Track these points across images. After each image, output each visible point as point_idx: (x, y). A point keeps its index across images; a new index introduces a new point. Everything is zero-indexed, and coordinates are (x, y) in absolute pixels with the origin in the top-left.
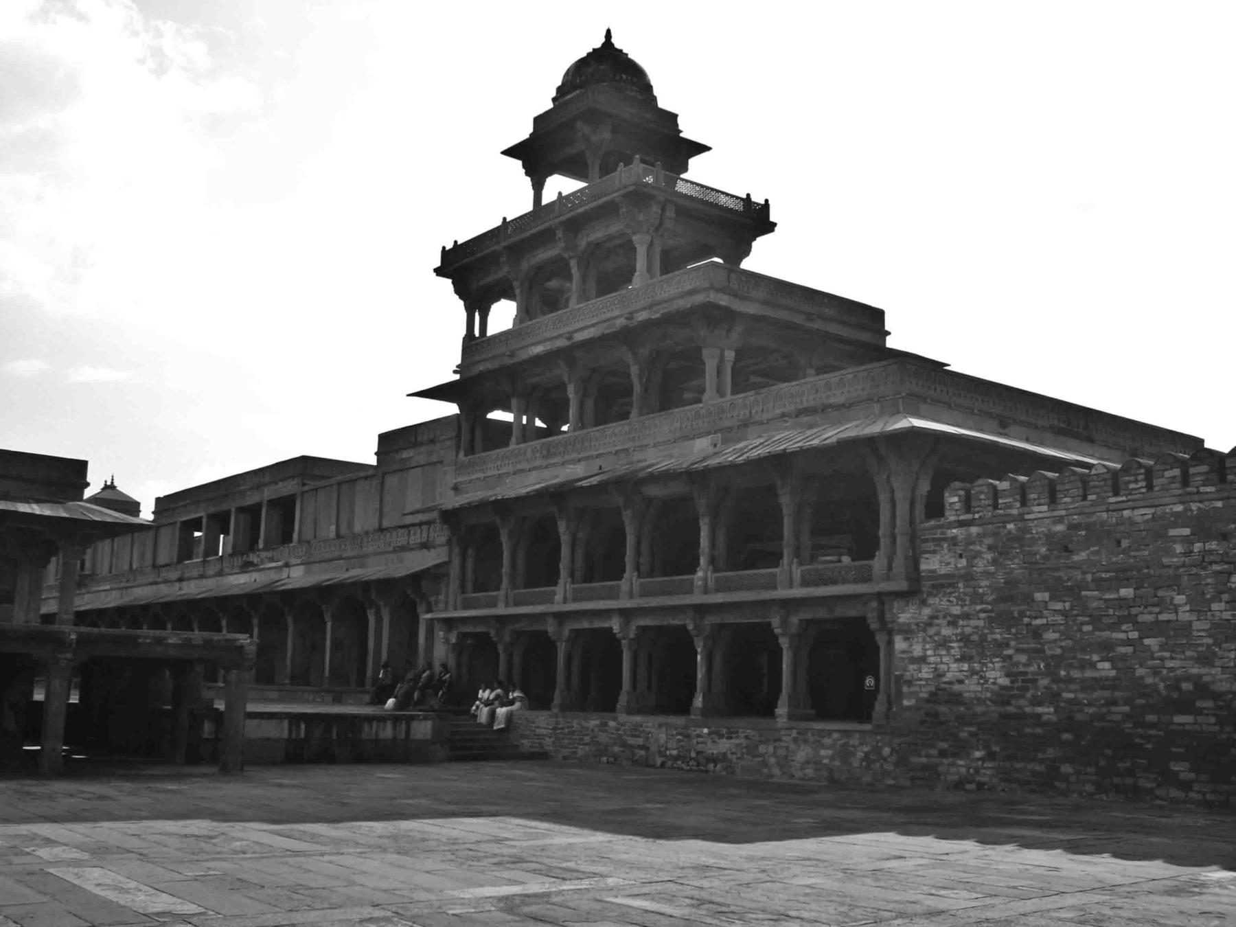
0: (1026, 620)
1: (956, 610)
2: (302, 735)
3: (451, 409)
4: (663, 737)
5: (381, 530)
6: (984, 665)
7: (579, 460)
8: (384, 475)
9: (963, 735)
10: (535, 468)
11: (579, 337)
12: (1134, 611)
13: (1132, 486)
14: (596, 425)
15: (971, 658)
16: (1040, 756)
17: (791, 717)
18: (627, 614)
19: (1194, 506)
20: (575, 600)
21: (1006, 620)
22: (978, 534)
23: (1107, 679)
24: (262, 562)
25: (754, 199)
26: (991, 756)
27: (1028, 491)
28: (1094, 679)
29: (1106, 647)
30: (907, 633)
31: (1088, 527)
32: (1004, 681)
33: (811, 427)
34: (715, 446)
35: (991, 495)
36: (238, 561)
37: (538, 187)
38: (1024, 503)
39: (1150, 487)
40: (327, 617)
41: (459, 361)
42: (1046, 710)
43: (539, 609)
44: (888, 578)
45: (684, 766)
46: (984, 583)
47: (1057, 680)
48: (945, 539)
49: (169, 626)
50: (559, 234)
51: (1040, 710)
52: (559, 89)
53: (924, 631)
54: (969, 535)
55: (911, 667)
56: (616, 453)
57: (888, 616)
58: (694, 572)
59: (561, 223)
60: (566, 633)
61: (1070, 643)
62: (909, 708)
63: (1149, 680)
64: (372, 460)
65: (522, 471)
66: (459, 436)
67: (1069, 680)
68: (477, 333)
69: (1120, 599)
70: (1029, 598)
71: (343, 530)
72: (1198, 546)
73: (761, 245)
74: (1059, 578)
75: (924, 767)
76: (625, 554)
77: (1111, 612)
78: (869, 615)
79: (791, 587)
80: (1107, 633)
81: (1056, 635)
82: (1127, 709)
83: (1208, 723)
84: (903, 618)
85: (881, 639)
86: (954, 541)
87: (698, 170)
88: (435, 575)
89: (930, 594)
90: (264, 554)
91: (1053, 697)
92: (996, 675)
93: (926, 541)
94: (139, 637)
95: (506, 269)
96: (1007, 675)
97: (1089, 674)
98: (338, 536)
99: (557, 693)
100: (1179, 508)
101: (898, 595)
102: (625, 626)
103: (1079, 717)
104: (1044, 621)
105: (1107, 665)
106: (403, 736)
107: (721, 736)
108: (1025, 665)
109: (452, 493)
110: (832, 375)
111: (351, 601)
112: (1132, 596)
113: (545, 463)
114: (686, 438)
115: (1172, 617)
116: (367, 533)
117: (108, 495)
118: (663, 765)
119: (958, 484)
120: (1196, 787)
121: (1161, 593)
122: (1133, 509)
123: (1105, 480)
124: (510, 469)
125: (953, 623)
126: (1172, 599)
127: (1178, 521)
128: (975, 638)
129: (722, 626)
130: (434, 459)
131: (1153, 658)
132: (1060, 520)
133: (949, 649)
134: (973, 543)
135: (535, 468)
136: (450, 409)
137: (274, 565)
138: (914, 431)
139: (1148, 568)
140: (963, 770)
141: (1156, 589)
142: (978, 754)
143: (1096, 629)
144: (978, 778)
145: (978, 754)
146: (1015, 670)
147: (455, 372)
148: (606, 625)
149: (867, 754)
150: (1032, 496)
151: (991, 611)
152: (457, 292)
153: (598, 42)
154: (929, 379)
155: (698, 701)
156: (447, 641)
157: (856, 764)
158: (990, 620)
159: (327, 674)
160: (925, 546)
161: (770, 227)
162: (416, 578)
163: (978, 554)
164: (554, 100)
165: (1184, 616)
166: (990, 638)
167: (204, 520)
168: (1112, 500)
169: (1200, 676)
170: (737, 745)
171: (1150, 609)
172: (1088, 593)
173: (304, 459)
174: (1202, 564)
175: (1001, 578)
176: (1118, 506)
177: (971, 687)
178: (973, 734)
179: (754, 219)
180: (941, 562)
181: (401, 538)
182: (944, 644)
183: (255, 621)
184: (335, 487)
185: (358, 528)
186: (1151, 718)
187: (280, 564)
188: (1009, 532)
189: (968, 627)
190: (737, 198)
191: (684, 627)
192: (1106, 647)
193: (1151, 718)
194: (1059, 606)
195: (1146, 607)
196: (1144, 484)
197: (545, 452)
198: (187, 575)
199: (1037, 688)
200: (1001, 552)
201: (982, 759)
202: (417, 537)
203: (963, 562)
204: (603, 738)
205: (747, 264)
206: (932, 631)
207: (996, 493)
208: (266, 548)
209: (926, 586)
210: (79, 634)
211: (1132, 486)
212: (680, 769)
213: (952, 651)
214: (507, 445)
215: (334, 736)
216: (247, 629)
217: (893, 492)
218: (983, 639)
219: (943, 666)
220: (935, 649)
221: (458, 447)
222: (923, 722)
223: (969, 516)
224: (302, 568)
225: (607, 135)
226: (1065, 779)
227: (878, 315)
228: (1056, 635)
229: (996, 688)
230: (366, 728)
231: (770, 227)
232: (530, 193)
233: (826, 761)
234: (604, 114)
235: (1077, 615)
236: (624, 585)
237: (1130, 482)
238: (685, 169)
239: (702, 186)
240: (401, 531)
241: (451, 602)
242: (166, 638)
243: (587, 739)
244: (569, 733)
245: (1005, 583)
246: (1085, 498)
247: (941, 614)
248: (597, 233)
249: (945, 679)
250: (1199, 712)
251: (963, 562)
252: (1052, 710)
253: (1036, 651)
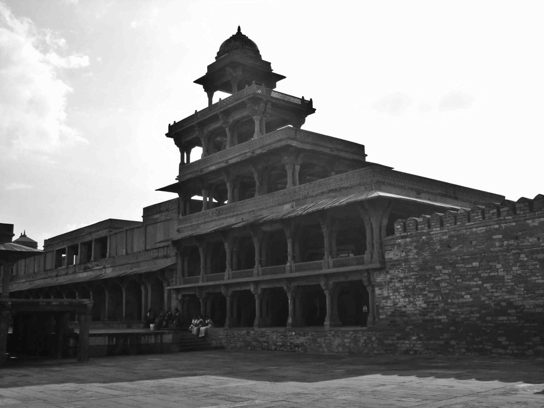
0: (432, 278)
1: (402, 275)
2: (114, 343)
3: (175, 196)
4: (274, 337)
5: (146, 250)
6: (415, 299)
7: (233, 216)
8: (146, 226)
9: (407, 330)
10: (215, 220)
11: (231, 162)
12: (479, 272)
13: (476, 217)
14: (240, 200)
15: (409, 296)
16: (441, 337)
17: (331, 325)
18: (257, 283)
19: (503, 225)
20: (233, 278)
22: (410, 242)
23: (469, 302)
24: (93, 267)
25: (305, 99)
26: (419, 339)
27: (431, 222)
28: (463, 303)
30: (381, 286)
31: (458, 236)
32: (424, 305)
33: (334, 197)
34: (293, 207)
35: (415, 225)
36: (82, 267)
37: (210, 97)
38: (429, 227)
39: (484, 218)
40: (123, 290)
41: (178, 174)
42: (443, 317)
43: (218, 283)
44: (371, 262)
45: (285, 350)
46: (413, 263)
48: (395, 244)
49: (52, 297)
50: (220, 117)
51: (440, 317)
52: (218, 53)
53: (388, 285)
54: (406, 243)
55: (383, 301)
56: (249, 212)
57: (372, 279)
58: (286, 263)
59: (221, 112)
60: (230, 292)
61: (452, 287)
62: (382, 319)
63: (487, 302)
64: (141, 220)
65: (207, 222)
66: (179, 207)
67: (452, 304)
68: (185, 162)
69: (473, 267)
70: (433, 268)
71: (129, 252)
72: (506, 243)
73: (309, 119)
74: (446, 260)
75: (390, 345)
76: (255, 257)
77: (469, 273)
78: (363, 279)
79: (329, 268)
80: (468, 283)
81: (446, 284)
82: (478, 315)
84: (379, 280)
85: (369, 289)
86: (399, 245)
87: (281, 87)
88: (171, 269)
89: (390, 269)
90: (93, 263)
91: (445, 311)
92: (420, 303)
93: (388, 245)
94: (40, 302)
95: (197, 133)
96: (425, 303)
97: (461, 300)
98: (127, 254)
99: (227, 319)
100: (497, 226)
101: (375, 270)
102: (256, 289)
103: (457, 320)
104: (440, 278)
105: (468, 296)
106: (159, 341)
107: (300, 335)
108: (433, 298)
109: (177, 233)
110: (342, 174)
111: (134, 283)
112: (478, 265)
113: (217, 218)
114: (280, 205)
115: (496, 274)
116: (140, 252)
117: (23, 239)
118: (275, 349)
119: (400, 220)
120: (510, 348)
121: (490, 264)
122: (477, 228)
123: (464, 215)
124: (203, 221)
125: (401, 281)
126: (495, 266)
127: (497, 232)
128: (411, 287)
129: (298, 287)
130: (168, 218)
131: (488, 292)
132: (445, 234)
133: (399, 292)
134: (408, 246)
135: (215, 220)
136: (174, 196)
137: (98, 268)
138: (380, 197)
139: (484, 253)
140: (408, 345)
141: (488, 262)
142: (414, 338)
143: (463, 281)
144: (414, 349)
145: (414, 338)
146: (428, 300)
147: (176, 179)
148: (247, 288)
149: (365, 340)
150: (433, 224)
151: (417, 275)
152: (176, 144)
153: (235, 32)
154: (385, 174)
155: (290, 320)
156: (177, 299)
157: (360, 344)
158: (416, 279)
159: (124, 315)
160: (387, 248)
161: (313, 111)
162: (162, 271)
163: (410, 250)
164: (216, 58)
165: (501, 273)
166: (417, 286)
167: (67, 249)
168: (468, 224)
169: (509, 299)
170: (308, 339)
171: (486, 271)
172: (459, 265)
173: (111, 220)
174: (508, 250)
175: (421, 261)
176: (471, 227)
177: (410, 309)
178: (411, 329)
179: (307, 108)
180: (394, 255)
181: (154, 254)
182: (396, 290)
183: (91, 293)
184: (143, 229)
185: (135, 250)
186: (489, 318)
187: (101, 267)
188: (424, 240)
189: (406, 282)
190: (298, 98)
191: (282, 288)
193: (489, 318)
194: (446, 271)
195: (484, 270)
196: (481, 216)
197: (217, 213)
198: (59, 274)
199: (439, 308)
200: (420, 248)
201: (416, 340)
202: (161, 253)
203: (404, 254)
204: (248, 338)
205: (303, 127)
206: (391, 285)
207: (417, 224)
208: (95, 260)
209: (388, 265)
210: (12, 302)
211: (476, 217)
212: (283, 350)
213: (401, 293)
214: (201, 210)
215: (129, 343)
216: (88, 297)
217: (372, 224)
218: (414, 287)
219: (397, 300)
220: (393, 293)
221: (179, 214)
222: (389, 325)
223: (406, 234)
224: (111, 269)
225: (240, 73)
226: (453, 346)
227: (362, 147)
228: (446, 284)
229: (421, 309)
230: (143, 338)
231: (313, 111)
232: (207, 99)
233: (347, 344)
234: (238, 63)
235: (454, 275)
236: (255, 271)
237: (475, 216)
238: (275, 87)
239: (283, 94)
240: (154, 251)
241: (178, 281)
242: (52, 302)
243: (241, 339)
244: (233, 337)
245: (423, 262)
246: (455, 224)
247: (395, 278)
248: (237, 116)
249: (398, 306)
250: (510, 315)
251: (404, 254)
252: (445, 317)
253: (437, 291)
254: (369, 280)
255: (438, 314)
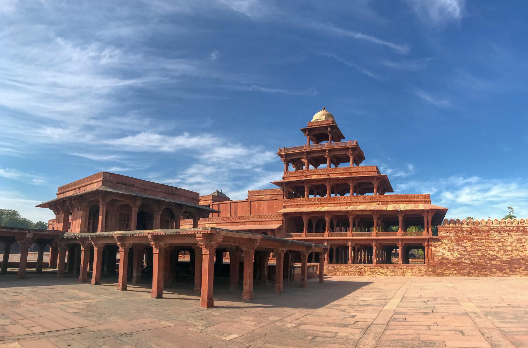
1: (447, 242)
21: (458, 245)
29: (480, 250)
47: (470, 256)
57: (430, 243)
67: (472, 256)
75: (440, 272)
83: (499, 263)
85: (426, 248)
86: (446, 230)
88: (279, 228)
125: (446, 245)
128: (451, 248)
129: (380, 244)
130: (274, 198)
132: (469, 228)
165: (494, 245)
177: (451, 257)
182: (444, 249)
186: (488, 262)
192: (480, 250)
203: (448, 234)
226: (472, 273)
254: (428, 243)
255: (465, 259)
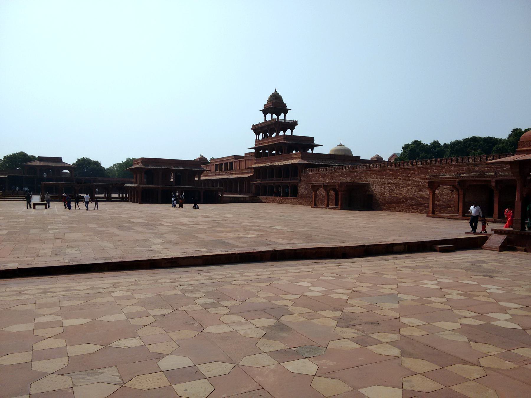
161: (298, 124)
227: (313, 138)
231: (298, 124)
234: (276, 105)
